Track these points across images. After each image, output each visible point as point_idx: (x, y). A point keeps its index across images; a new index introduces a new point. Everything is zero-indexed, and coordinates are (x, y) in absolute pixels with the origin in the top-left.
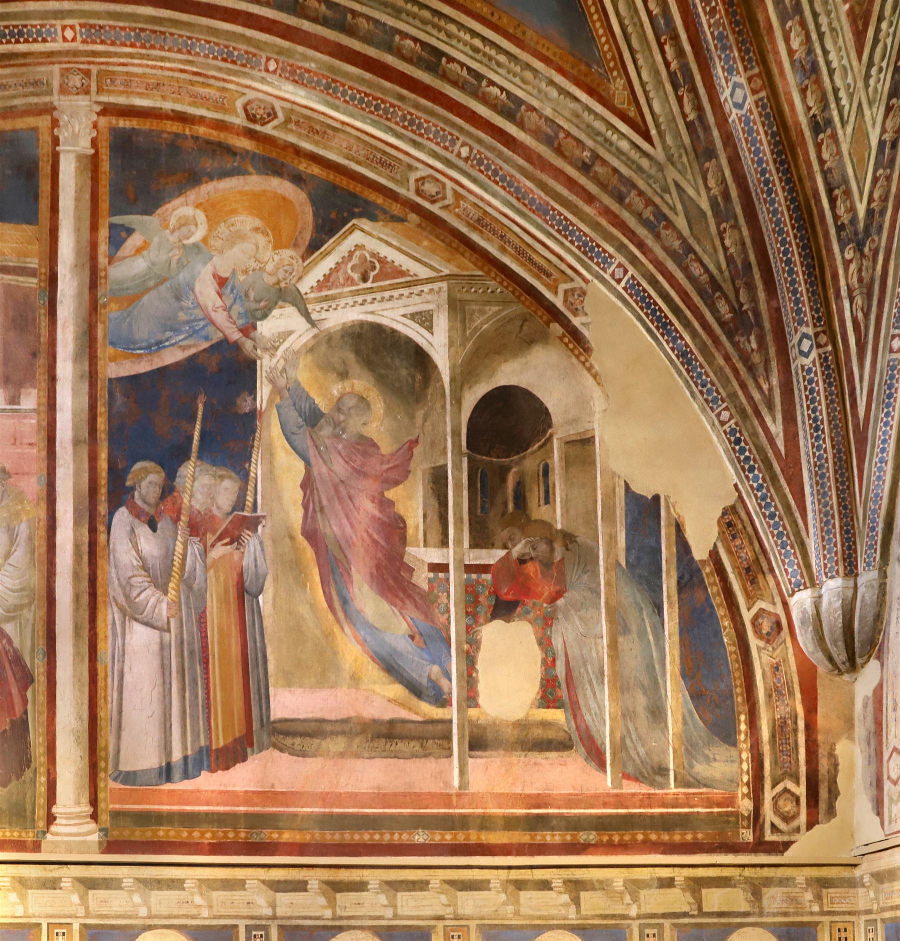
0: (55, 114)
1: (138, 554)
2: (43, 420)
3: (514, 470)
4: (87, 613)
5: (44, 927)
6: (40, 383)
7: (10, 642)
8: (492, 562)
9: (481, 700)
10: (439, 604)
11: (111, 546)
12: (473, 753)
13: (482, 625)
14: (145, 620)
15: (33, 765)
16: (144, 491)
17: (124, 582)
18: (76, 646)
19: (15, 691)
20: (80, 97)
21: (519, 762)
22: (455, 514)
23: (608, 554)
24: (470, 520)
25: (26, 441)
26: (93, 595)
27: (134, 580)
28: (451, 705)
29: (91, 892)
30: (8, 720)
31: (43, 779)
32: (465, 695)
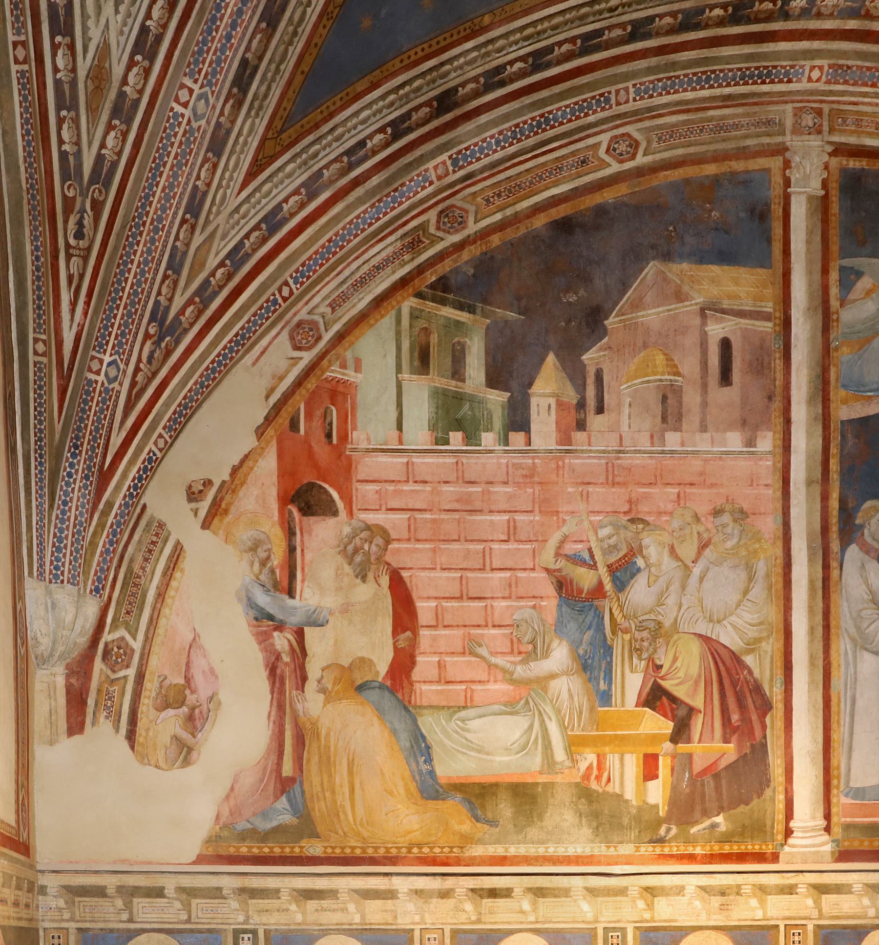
0: (788, 155)
1: (869, 588)
2: (779, 462)
4: (821, 644)
5: (782, 928)
6: (776, 426)
7: (750, 672)
11: (843, 581)
14: (875, 649)
15: (772, 784)
16: (873, 528)
17: (855, 615)
18: (811, 674)
19: (754, 717)
20: (812, 137)
25: (763, 482)
26: (827, 627)
27: (864, 612)
29: (824, 897)
30: (748, 744)
31: (781, 797)
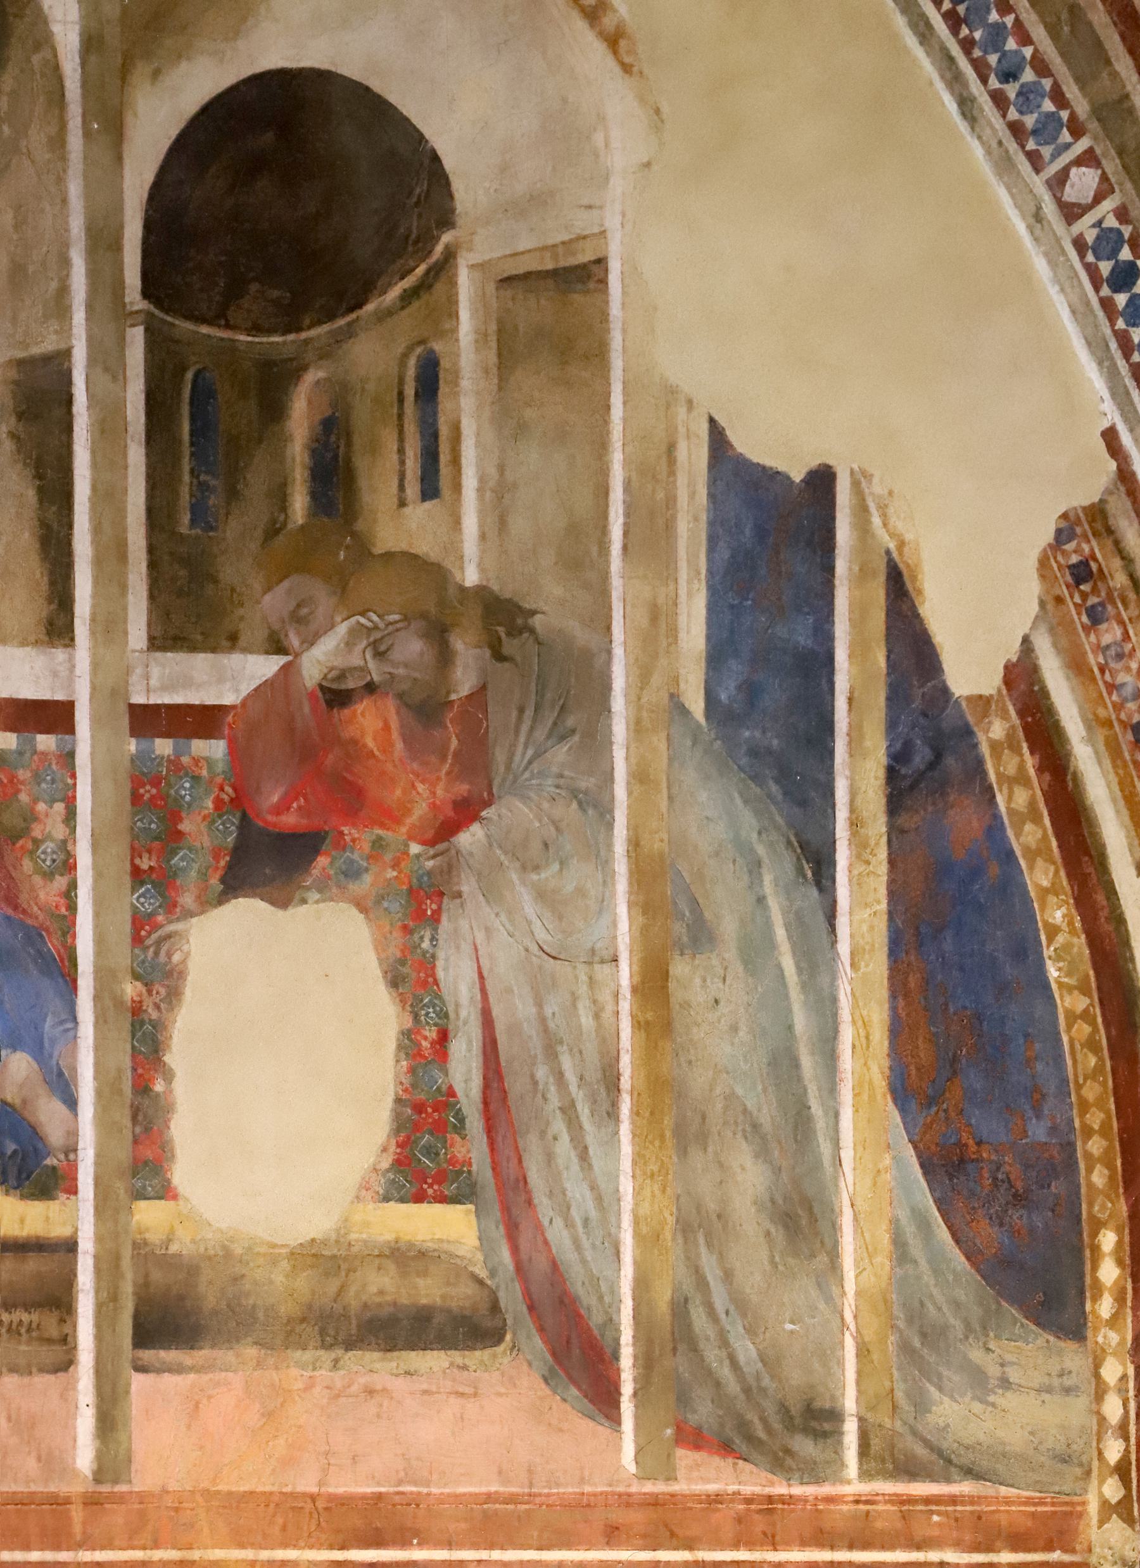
3: (312, 376)
8: (229, 699)
9: (180, 1175)
10: (37, 843)
12: (148, 1355)
13: (189, 914)
21: (308, 1388)
22: (97, 529)
23: (642, 674)
24: (151, 550)
28: (73, 1191)
32: (123, 1153)
